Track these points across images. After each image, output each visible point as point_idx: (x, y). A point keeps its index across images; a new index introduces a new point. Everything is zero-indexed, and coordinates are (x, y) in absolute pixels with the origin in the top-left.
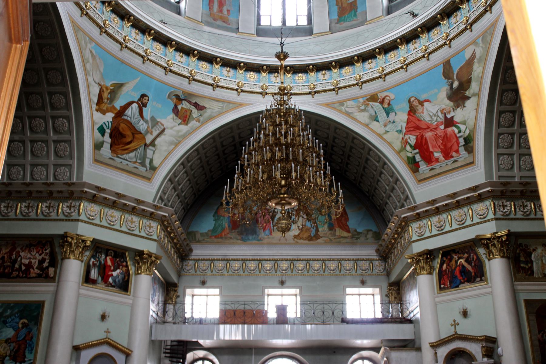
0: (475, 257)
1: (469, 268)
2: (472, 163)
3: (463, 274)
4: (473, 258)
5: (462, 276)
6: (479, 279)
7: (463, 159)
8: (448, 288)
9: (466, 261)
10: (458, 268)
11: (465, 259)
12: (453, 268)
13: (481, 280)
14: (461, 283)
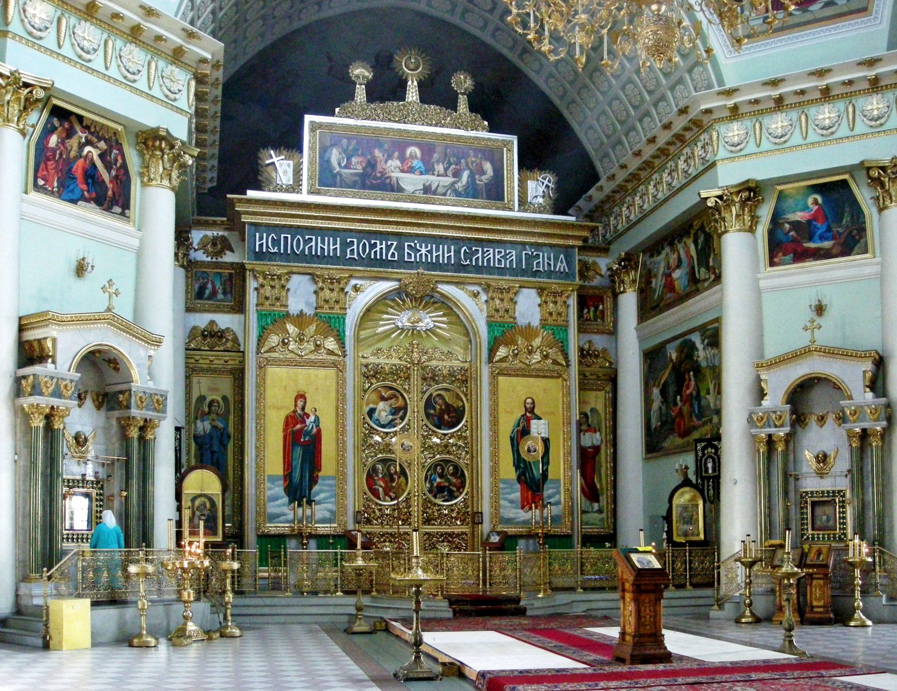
0: (120, 161)
1: (106, 176)
3: (90, 181)
4: (116, 160)
5: (88, 184)
6: (118, 209)
8: (52, 193)
9: (102, 156)
10: (82, 160)
11: (99, 152)
12: (73, 154)
13: (123, 214)
14: (83, 198)
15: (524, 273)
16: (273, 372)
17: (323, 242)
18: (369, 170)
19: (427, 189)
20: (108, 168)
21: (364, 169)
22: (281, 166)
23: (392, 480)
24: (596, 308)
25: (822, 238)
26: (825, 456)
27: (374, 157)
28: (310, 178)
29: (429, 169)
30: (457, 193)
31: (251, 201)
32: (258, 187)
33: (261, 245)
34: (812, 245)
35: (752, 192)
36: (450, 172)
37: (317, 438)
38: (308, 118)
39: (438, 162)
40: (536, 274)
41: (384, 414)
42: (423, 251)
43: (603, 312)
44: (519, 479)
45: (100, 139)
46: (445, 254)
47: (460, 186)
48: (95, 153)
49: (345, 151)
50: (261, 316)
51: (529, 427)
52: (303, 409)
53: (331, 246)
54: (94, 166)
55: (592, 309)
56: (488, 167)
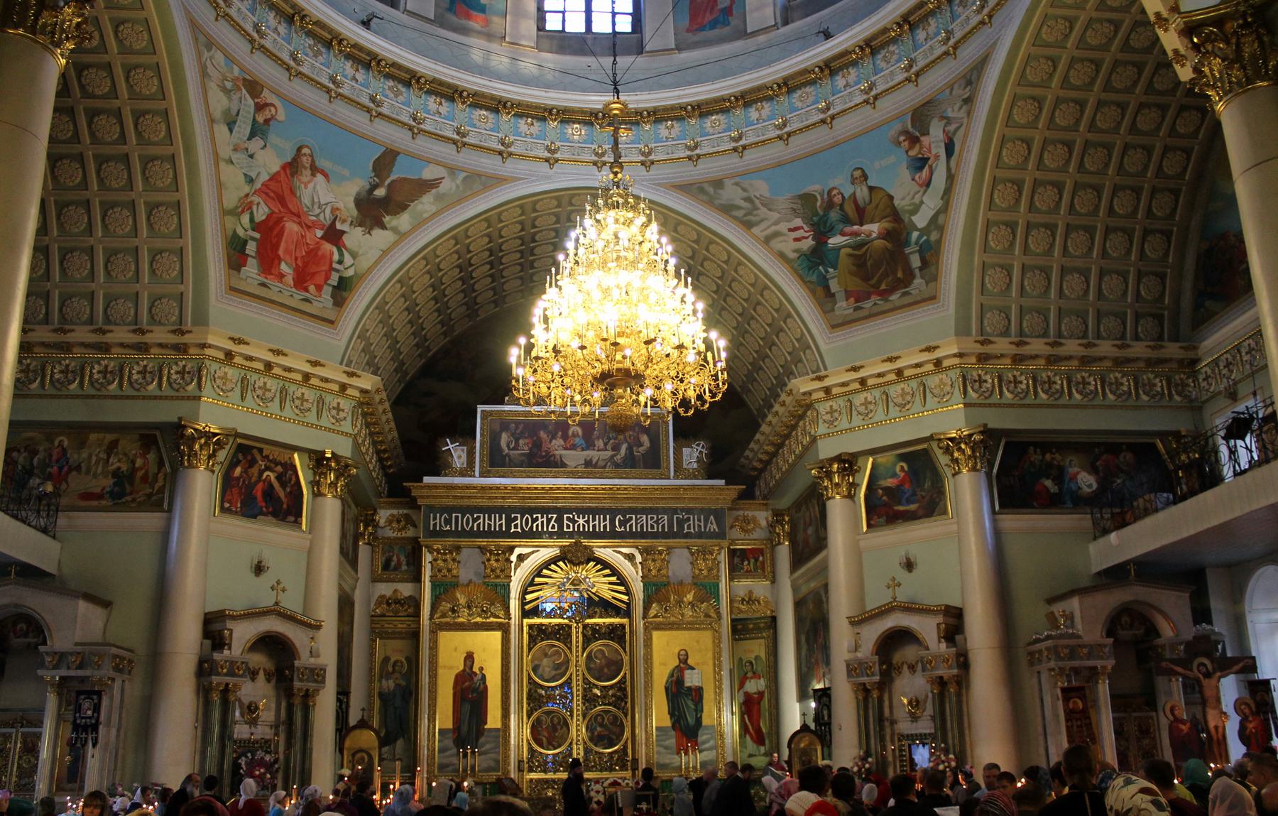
1: (282, 494)
2: (332, 322)
6: (292, 519)
7: (321, 305)
9: (279, 478)
12: (253, 480)
13: (296, 522)
15: (675, 536)
16: (446, 638)
17: (490, 519)
18: (535, 450)
19: (588, 463)
20: (283, 485)
21: (530, 449)
22: (457, 453)
23: (555, 730)
24: (757, 560)
25: (909, 502)
26: (917, 701)
27: (539, 439)
28: (481, 461)
29: (589, 445)
30: (617, 466)
31: (430, 487)
32: (436, 473)
33: (435, 525)
34: (901, 508)
35: (848, 463)
36: (609, 447)
37: (483, 694)
38: (480, 408)
39: (598, 438)
40: (688, 536)
41: (547, 669)
42: (581, 521)
43: (763, 563)
44: (674, 727)
45: (277, 464)
46: (601, 523)
47: (618, 458)
48: (272, 476)
49: (513, 435)
50: (435, 586)
51: (683, 676)
52: (471, 667)
53: (499, 522)
54: (271, 486)
55: (752, 561)
56: (645, 439)
